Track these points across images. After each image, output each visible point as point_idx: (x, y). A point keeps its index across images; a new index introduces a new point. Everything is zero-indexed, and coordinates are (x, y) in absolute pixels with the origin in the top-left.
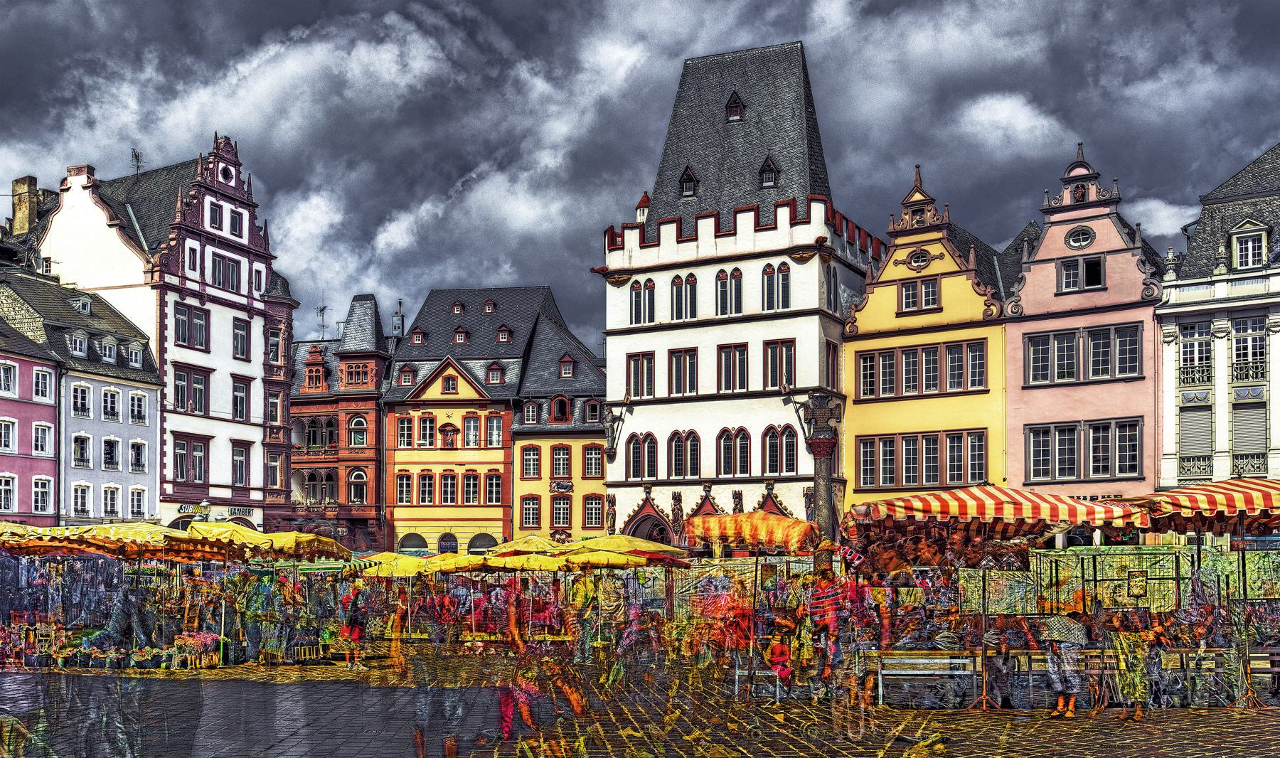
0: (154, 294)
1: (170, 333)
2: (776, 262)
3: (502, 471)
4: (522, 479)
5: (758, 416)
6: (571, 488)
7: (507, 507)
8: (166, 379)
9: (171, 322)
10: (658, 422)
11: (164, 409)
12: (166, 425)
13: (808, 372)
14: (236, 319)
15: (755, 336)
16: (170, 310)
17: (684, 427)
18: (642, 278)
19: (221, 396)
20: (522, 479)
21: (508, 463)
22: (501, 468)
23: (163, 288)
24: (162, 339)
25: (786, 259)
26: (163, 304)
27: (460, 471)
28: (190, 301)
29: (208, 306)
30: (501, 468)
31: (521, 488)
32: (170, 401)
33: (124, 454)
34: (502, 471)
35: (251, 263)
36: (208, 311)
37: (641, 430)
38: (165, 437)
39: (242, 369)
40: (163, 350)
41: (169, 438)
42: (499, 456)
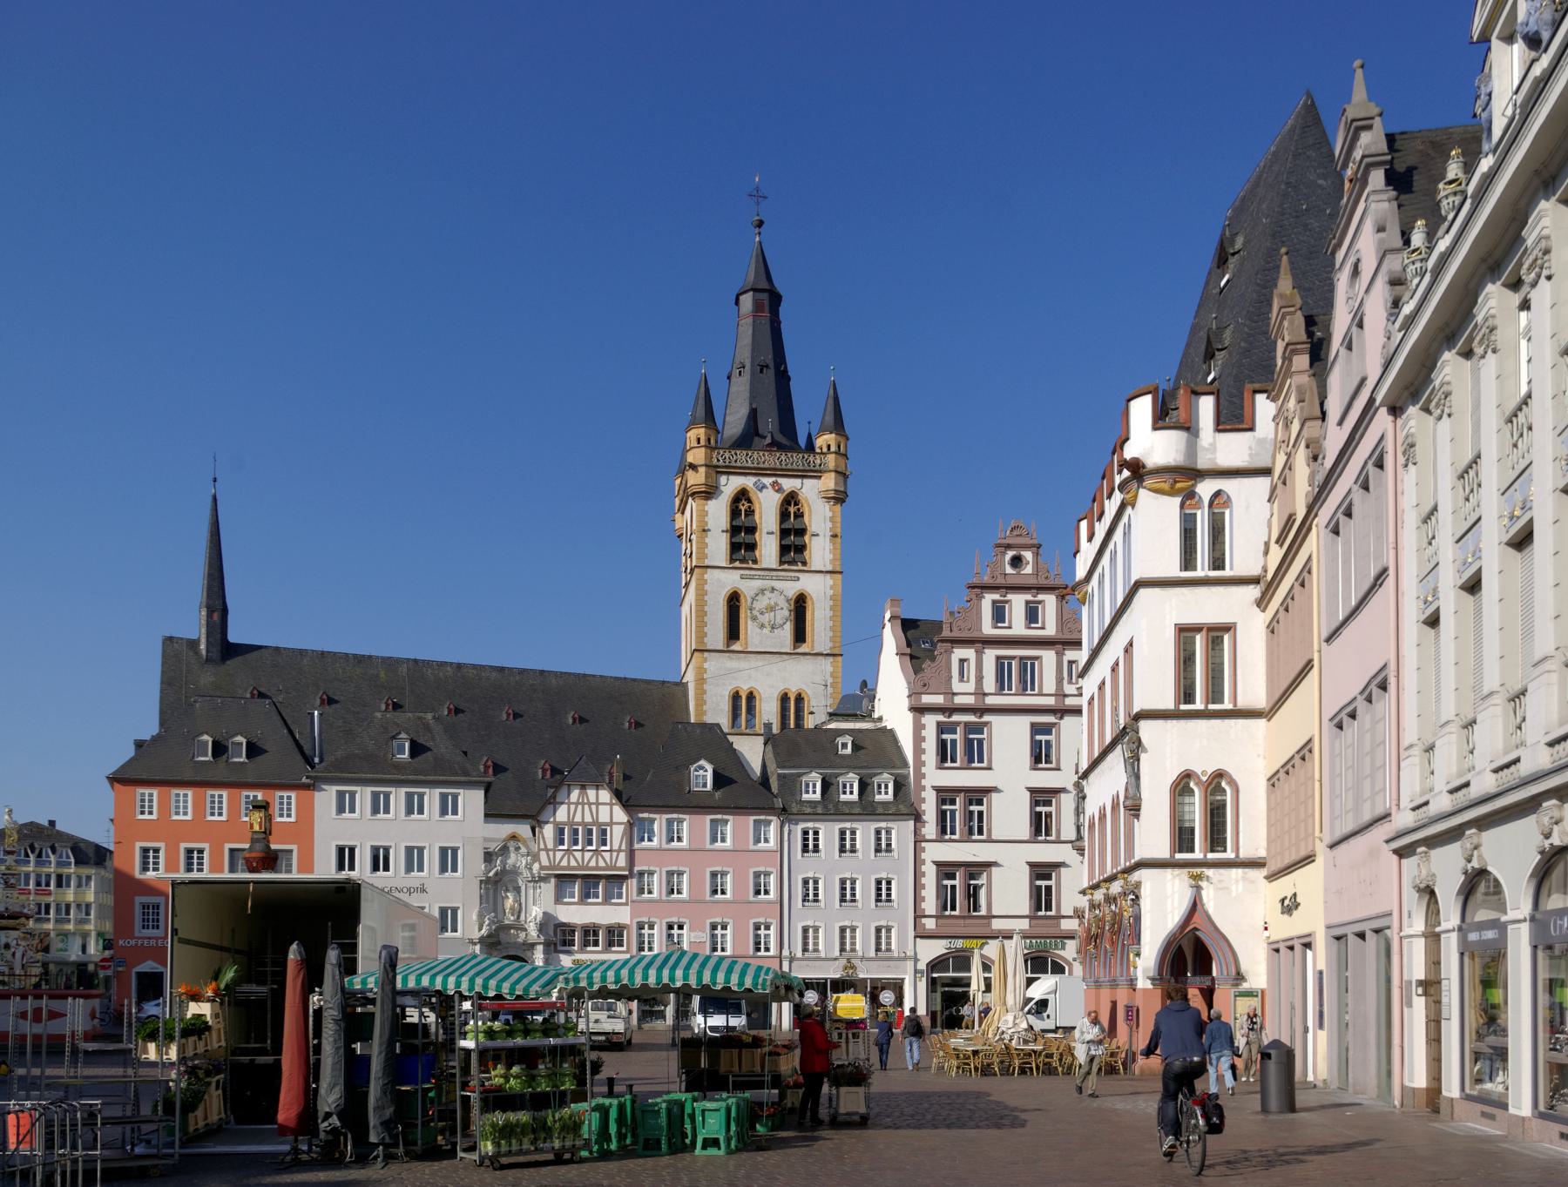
0: (910, 716)
1: (931, 756)
8: (924, 807)
9: (930, 746)
11: (919, 840)
12: (923, 856)
14: (1033, 725)
16: (930, 734)
19: (1009, 813)
23: (919, 710)
24: (919, 763)
26: (918, 728)
28: (956, 718)
29: (986, 718)
32: (930, 830)
33: (864, 891)
35: (1060, 655)
36: (986, 724)
38: (923, 868)
39: (1045, 779)
40: (920, 776)
41: (930, 872)
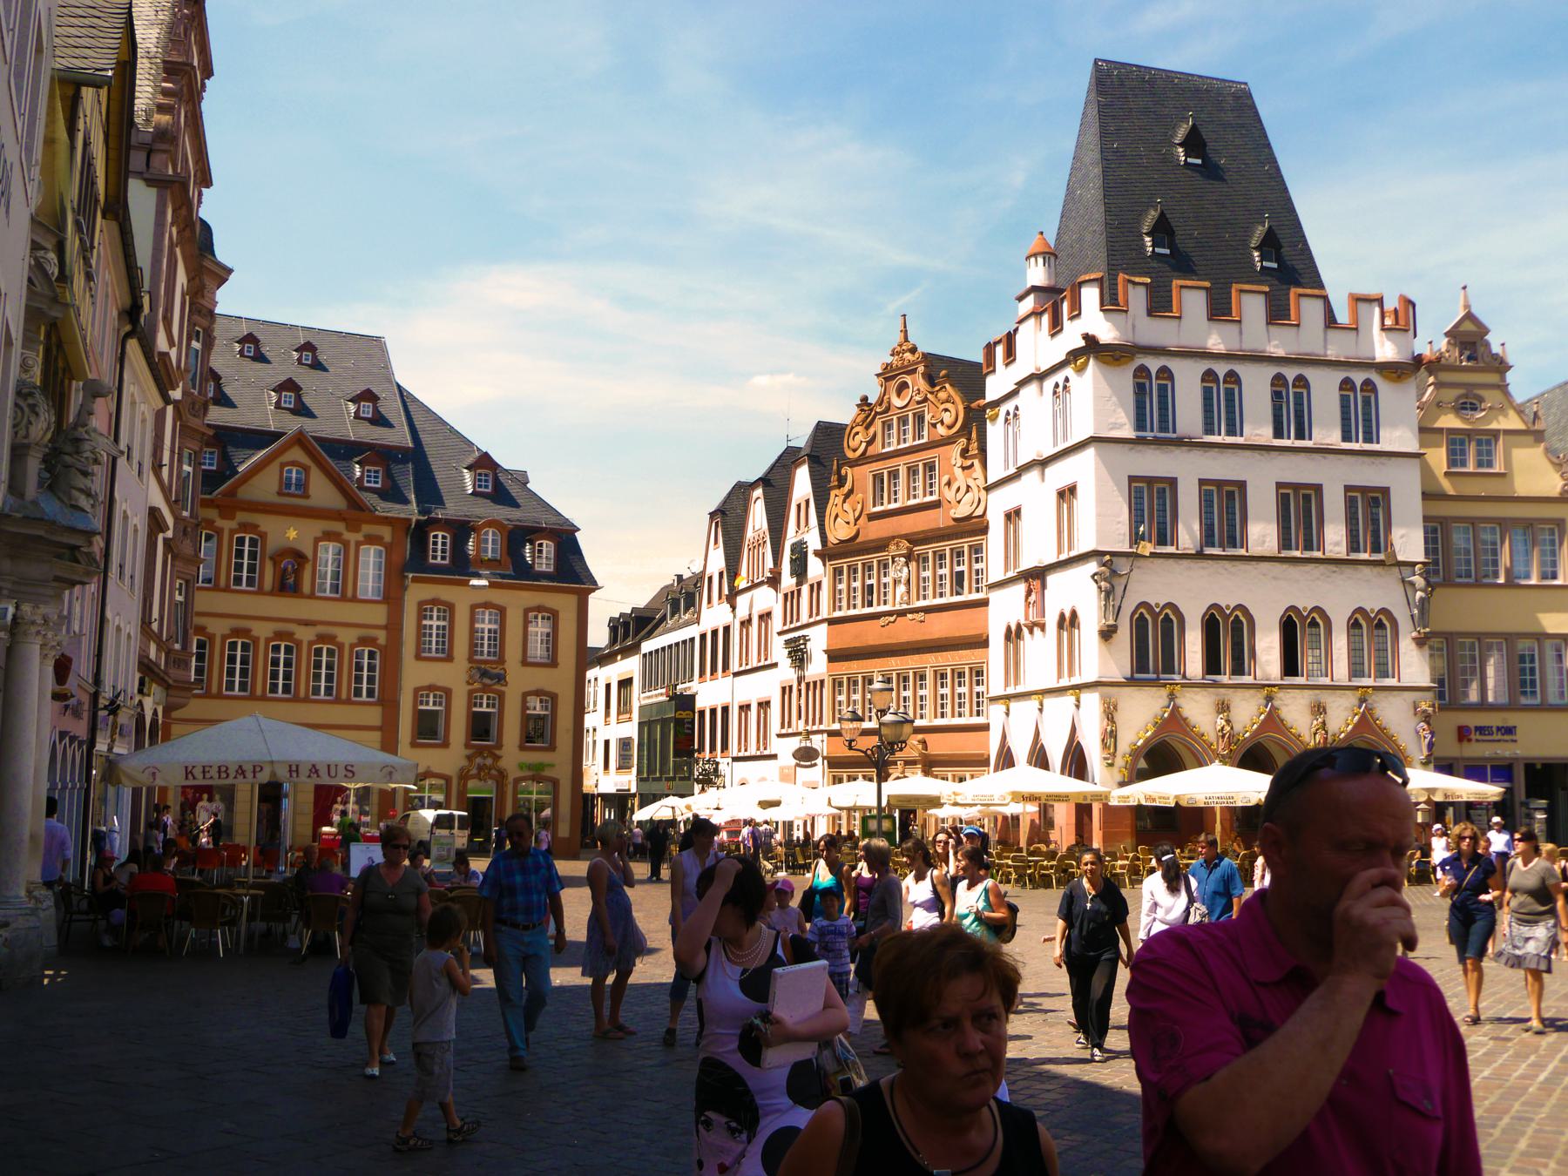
2: (1358, 377)
3: (382, 640)
4: (418, 657)
5: (1339, 596)
6: (501, 678)
7: (389, 704)
10: (1192, 591)
13: (1409, 543)
15: (1333, 480)
17: (1228, 600)
18: (1154, 364)
20: (418, 657)
21: (394, 626)
22: (382, 637)
25: (1375, 377)
27: (305, 635)
30: (382, 637)
31: (414, 674)
34: (382, 640)
37: (1157, 598)
42: (379, 615)
